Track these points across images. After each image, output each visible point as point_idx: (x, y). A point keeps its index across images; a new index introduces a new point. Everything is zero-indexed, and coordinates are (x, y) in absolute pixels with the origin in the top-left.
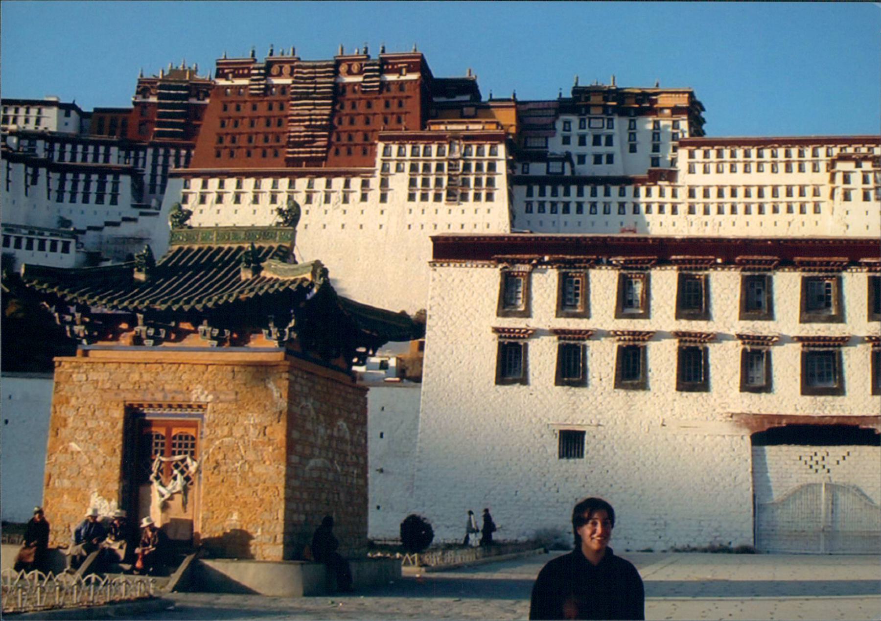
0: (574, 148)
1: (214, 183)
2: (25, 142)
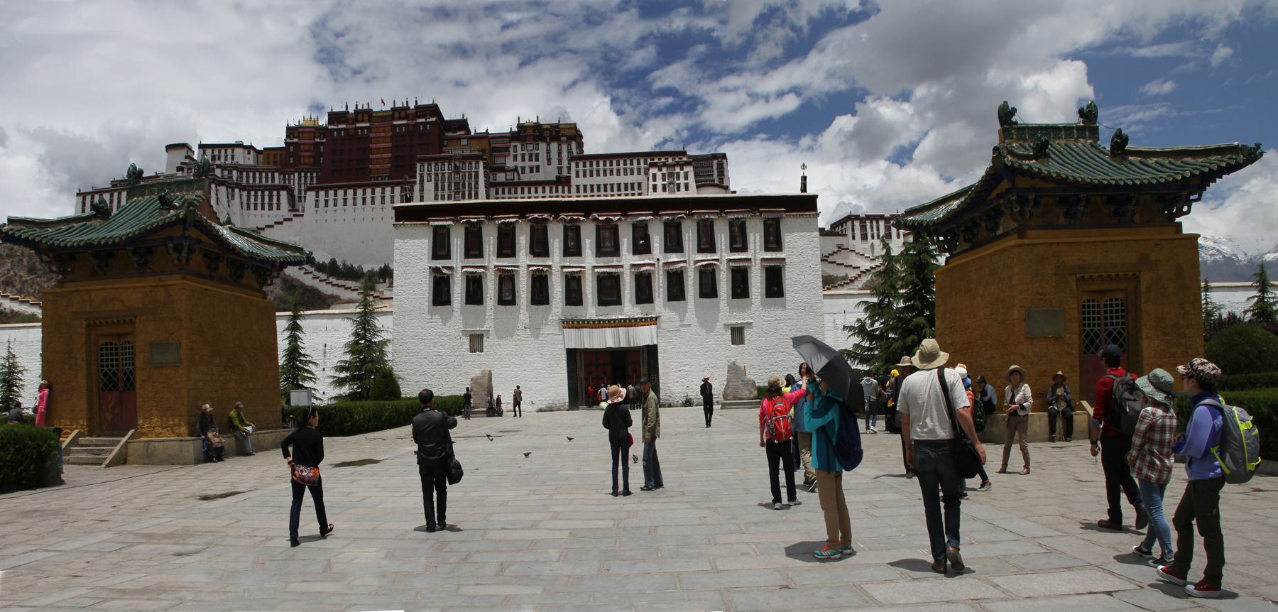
0: (519, 164)
1: (331, 193)
2: (226, 173)
